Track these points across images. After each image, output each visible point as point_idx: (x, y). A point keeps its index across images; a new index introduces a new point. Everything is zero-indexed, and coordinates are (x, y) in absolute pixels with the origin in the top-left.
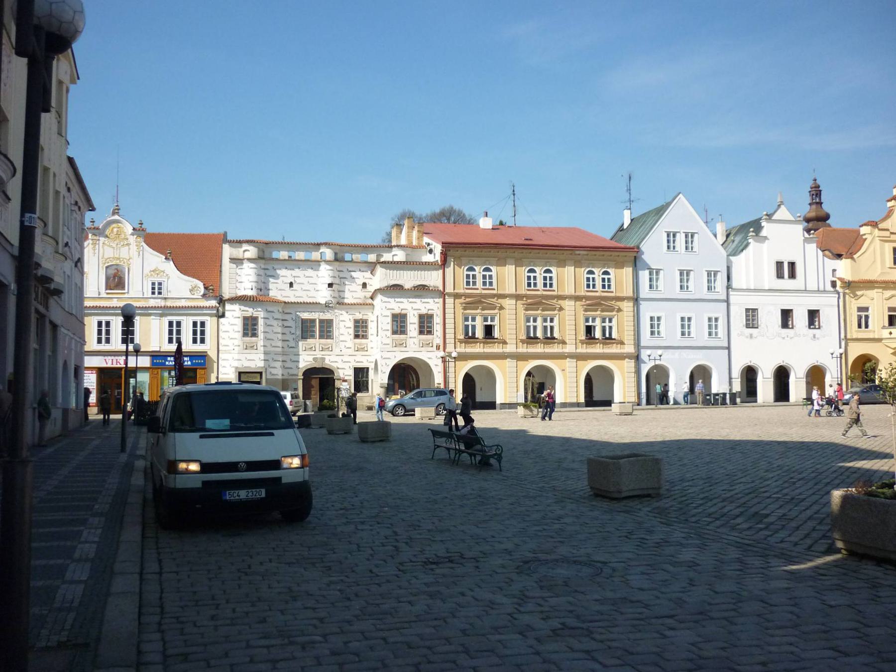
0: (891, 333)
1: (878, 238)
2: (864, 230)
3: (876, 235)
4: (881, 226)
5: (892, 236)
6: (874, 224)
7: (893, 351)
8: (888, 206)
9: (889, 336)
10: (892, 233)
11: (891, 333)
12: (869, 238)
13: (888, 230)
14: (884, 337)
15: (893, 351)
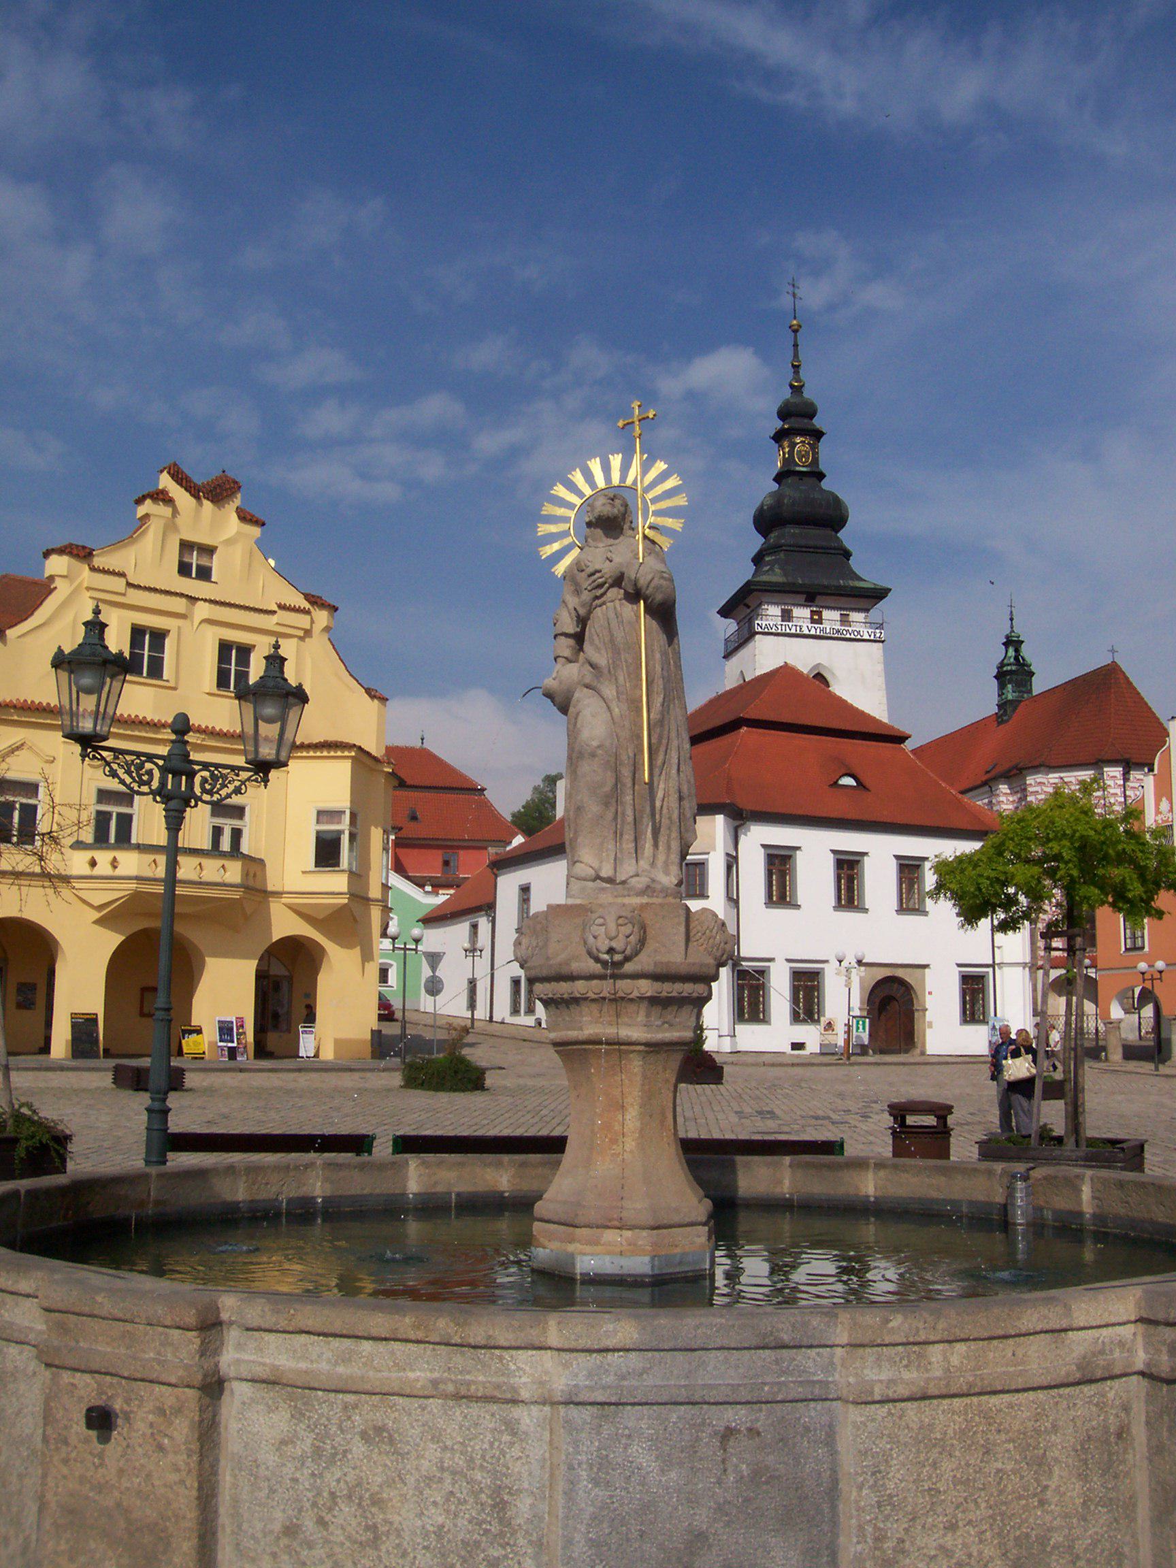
0: (93, 863)
1: (88, 594)
2: (57, 565)
3: (85, 585)
4: (98, 561)
5: (131, 591)
6: (83, 554)
7: (97, 915)
8: (139, 516)
9: (87, 871)
10: (129, 585)
11: (93, 863)
12: (62, 589)
13: (122, 575)
14: (75, 872)
15: (97, 915)
